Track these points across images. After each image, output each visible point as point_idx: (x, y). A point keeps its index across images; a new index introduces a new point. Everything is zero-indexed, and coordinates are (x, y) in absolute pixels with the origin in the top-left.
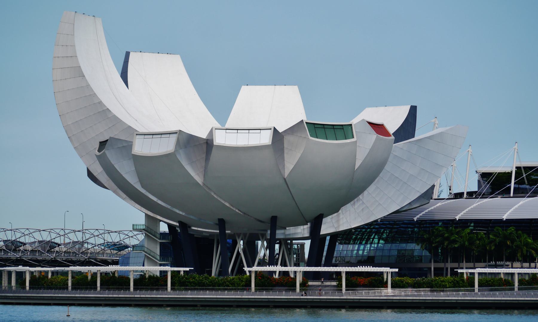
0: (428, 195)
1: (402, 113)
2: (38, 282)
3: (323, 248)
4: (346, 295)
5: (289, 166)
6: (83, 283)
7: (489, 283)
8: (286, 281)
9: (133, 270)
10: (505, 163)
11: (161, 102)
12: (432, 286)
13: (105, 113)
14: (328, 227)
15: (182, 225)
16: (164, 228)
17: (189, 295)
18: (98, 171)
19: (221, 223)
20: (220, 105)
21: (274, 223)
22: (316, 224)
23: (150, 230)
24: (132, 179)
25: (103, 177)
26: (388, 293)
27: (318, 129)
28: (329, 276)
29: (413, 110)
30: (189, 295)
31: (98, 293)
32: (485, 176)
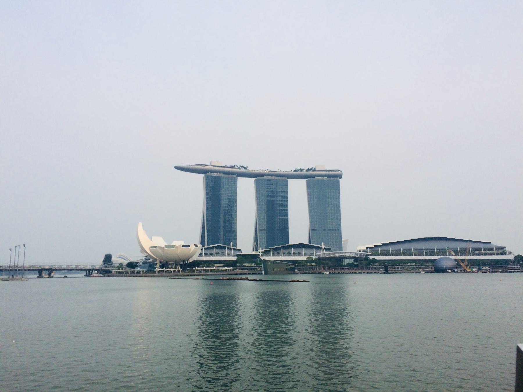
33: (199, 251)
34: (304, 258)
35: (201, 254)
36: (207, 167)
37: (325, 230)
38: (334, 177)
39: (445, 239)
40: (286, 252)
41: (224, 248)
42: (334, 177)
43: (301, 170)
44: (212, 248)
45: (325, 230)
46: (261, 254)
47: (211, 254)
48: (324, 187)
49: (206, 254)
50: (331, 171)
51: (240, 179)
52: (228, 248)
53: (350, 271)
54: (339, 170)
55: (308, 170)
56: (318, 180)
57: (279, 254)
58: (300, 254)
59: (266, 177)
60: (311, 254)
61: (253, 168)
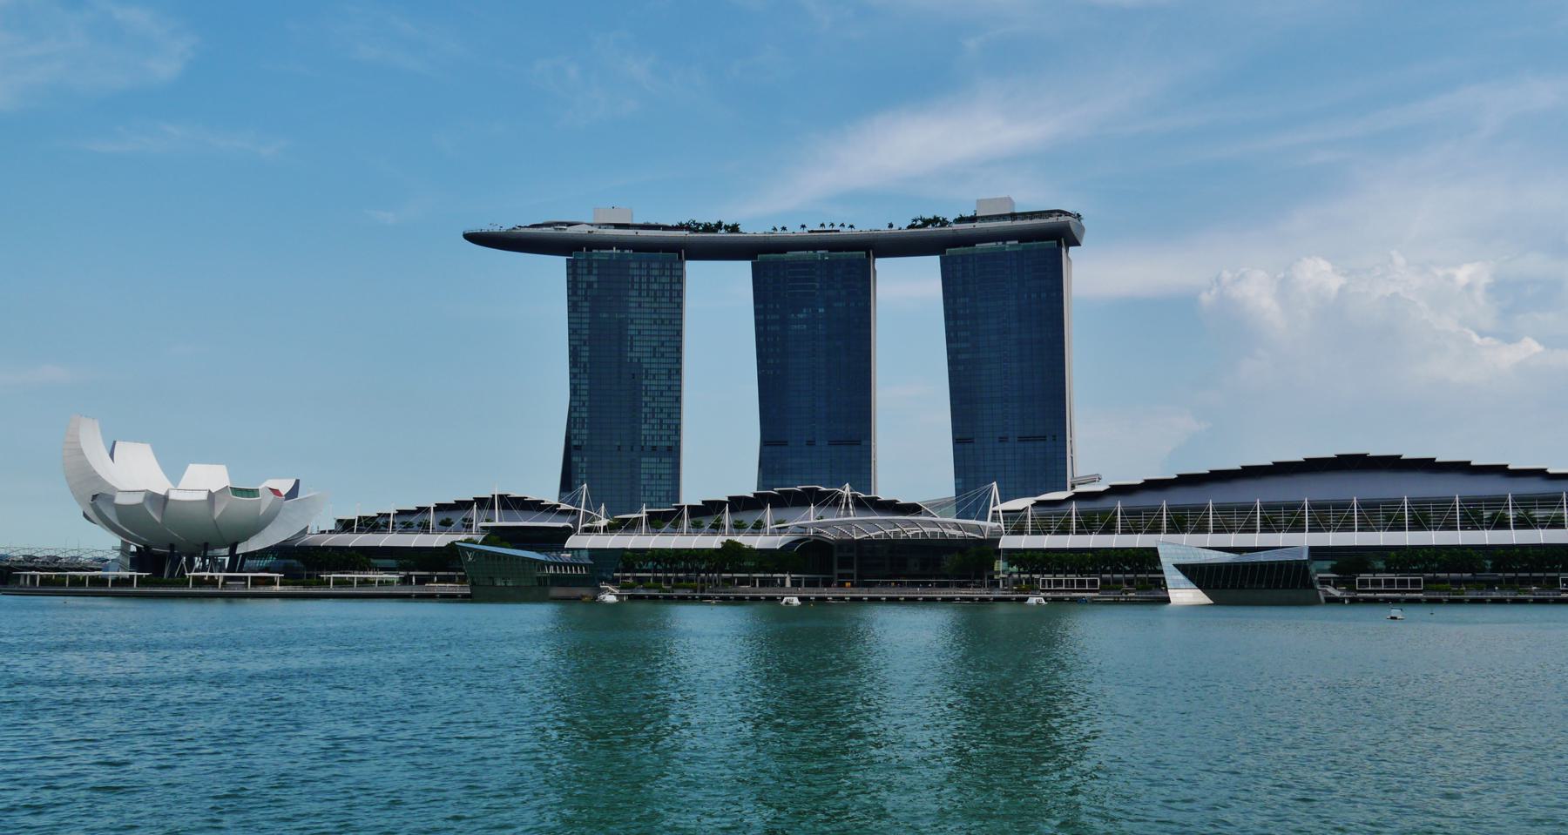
0: (304, 531)
1: (291, 483)
2: (45, 581)
3: (237, 562)
4: (250, 590)
5: (217, 513)
6: (76, 582)
7: (338, 583)
8: (213, 582)
9: (111, 574)
10: (352, 514)
11: (135, 473)
12: (305, 585)
13: (96, 478)
14: (240, 550)
15: (146, 547)
16: (133, 549)
17: (148, 590)
18: (91, 513)
19: (172, 547)
20: (174, 472)
21: (206, 546)
22: (233, 547)
23: (124, 550)
24: (114, 519)
25: (94, 517)
26: (277, 588)
27: (237, 491)
28: (240, 579)
29: (297, 482)
30: (148, 590)
31: (87, 589)
32: (339, 521)
34: (715, 542)
36: (571, 230)
37: (1003, 440)
38: (1050, 239)
39: (1393, 464)
42: (1050, 239)
45: (1003, 440)
48: (1009, 280)
50: (1032, 215)
51: (694, 270)
53: (919, 593)
54: (1061, 213)
56: (985, 257)
57: (676, 527)
58: (758, 527)
59: (790, 254)
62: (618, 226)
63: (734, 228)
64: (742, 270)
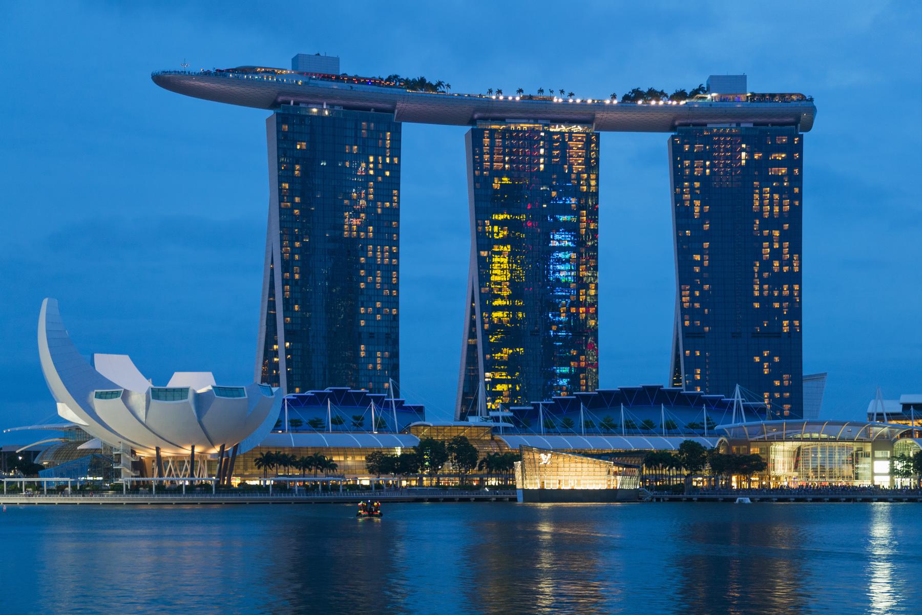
33: (274, 416)
34: (671, 444)
35: (279, 425)
40: (598, 419)
41: (364, 401)
43: (654, 94)
44: (319, 400)
46: (502, 424)
47: (317, 425)
49: (296, 425)
52: (379, 401)
54: (802, 98)
55: (680, 95)
58: (648, 428)
60: (692, 426)
61: (464, 84)
62: (327, 77)
63: (434, 88)
64: (456, 137)
